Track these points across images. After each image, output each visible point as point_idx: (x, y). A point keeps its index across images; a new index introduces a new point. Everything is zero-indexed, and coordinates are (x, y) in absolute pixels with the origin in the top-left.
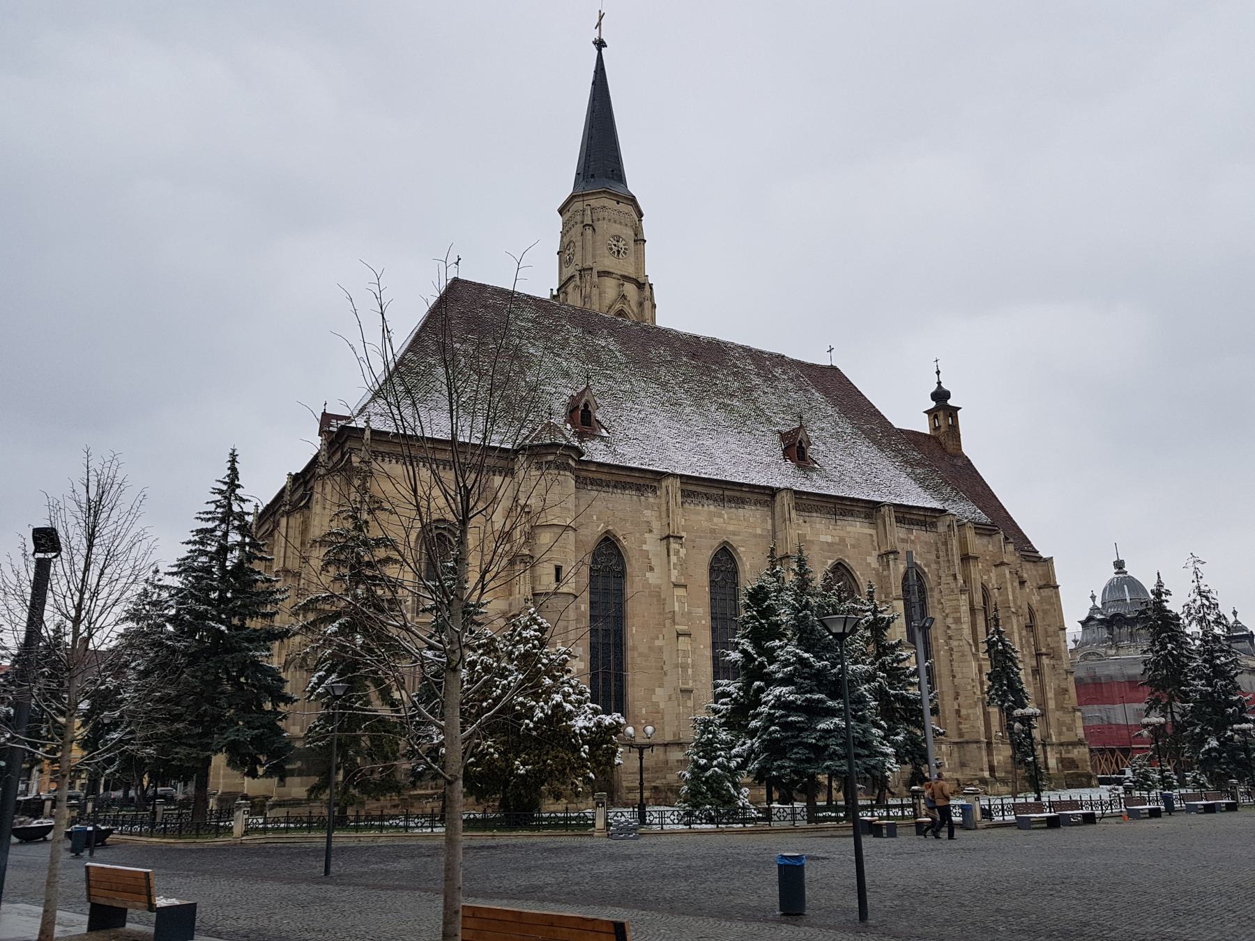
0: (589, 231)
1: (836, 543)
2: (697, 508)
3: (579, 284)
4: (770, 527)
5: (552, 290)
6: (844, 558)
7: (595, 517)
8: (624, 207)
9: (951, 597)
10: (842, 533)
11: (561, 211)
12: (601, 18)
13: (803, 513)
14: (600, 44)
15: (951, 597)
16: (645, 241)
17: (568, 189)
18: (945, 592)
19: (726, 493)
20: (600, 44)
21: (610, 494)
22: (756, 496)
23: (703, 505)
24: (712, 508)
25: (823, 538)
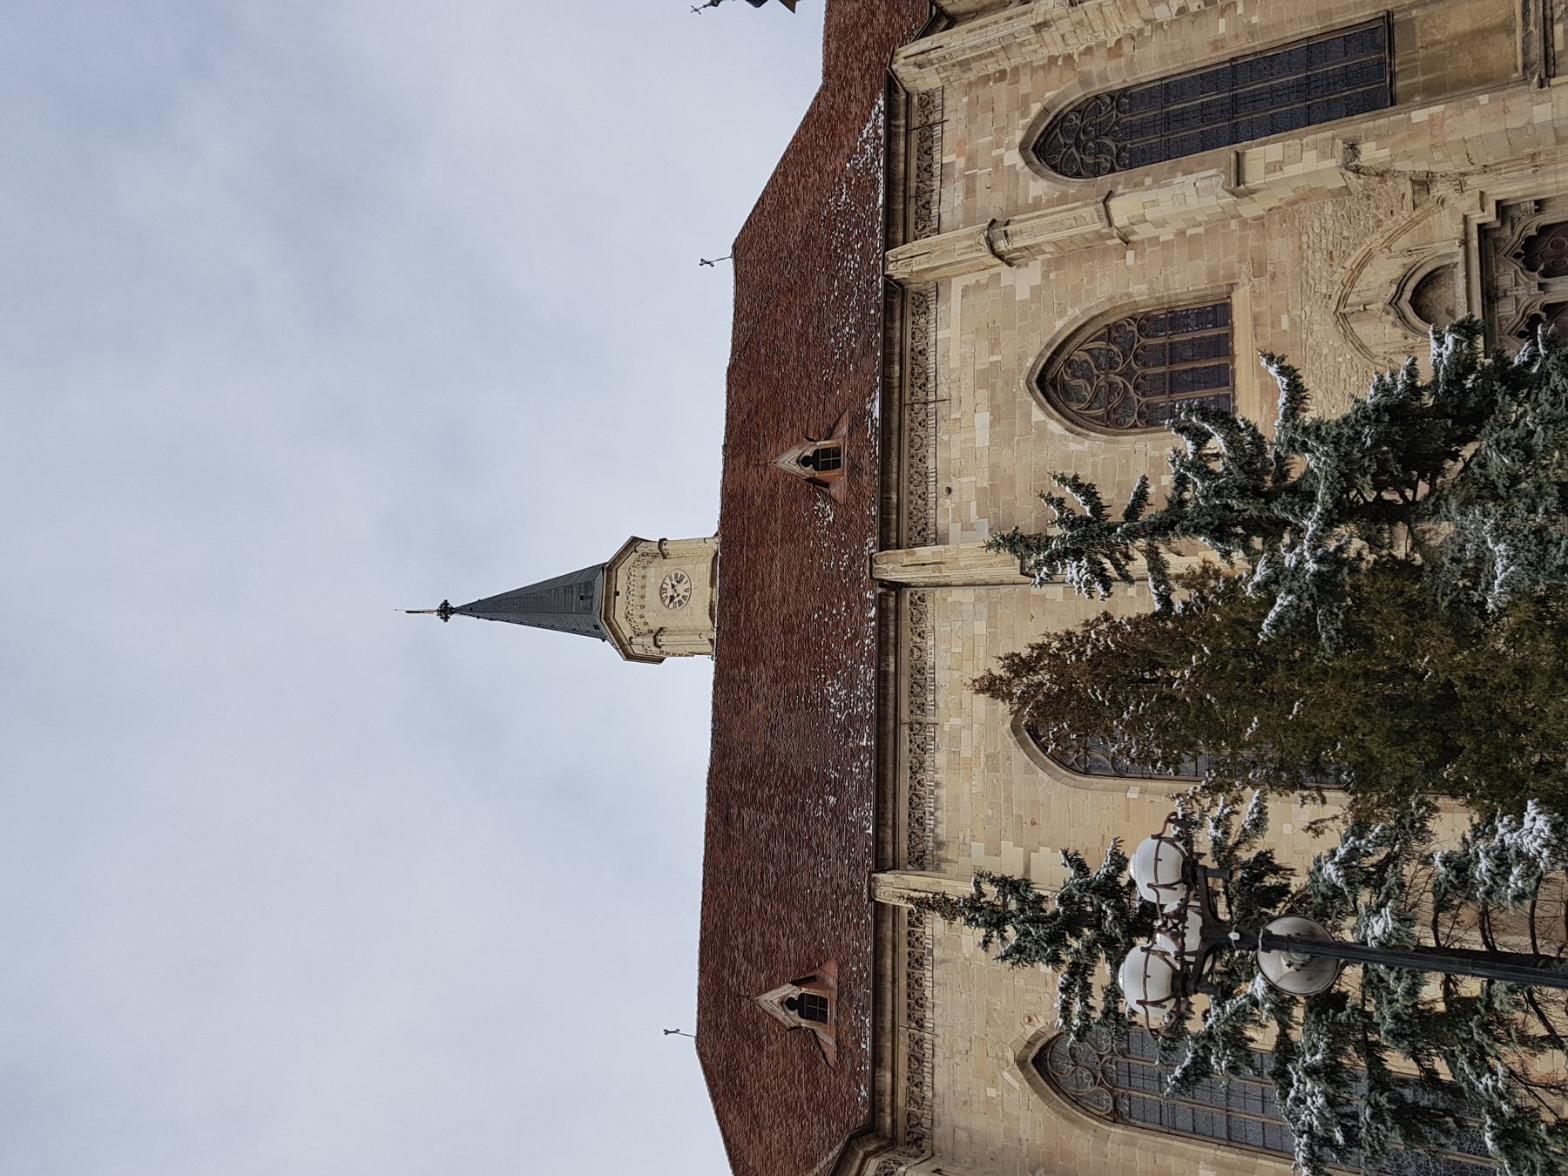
1: (992, 398)
2: (943, 800)
4: (967, 595)
6: (1025, 373)
7: (991, 1092)
9: (1098, 24)
10: (968, 381)
13: (931, 503)
15: (1098, 24)
18: (1087, 40)
19: (905, 715)
21: (938, 1041)
22: (906, 633)
23: (937, 785)
24: (941, 759)
25: (982, 437)
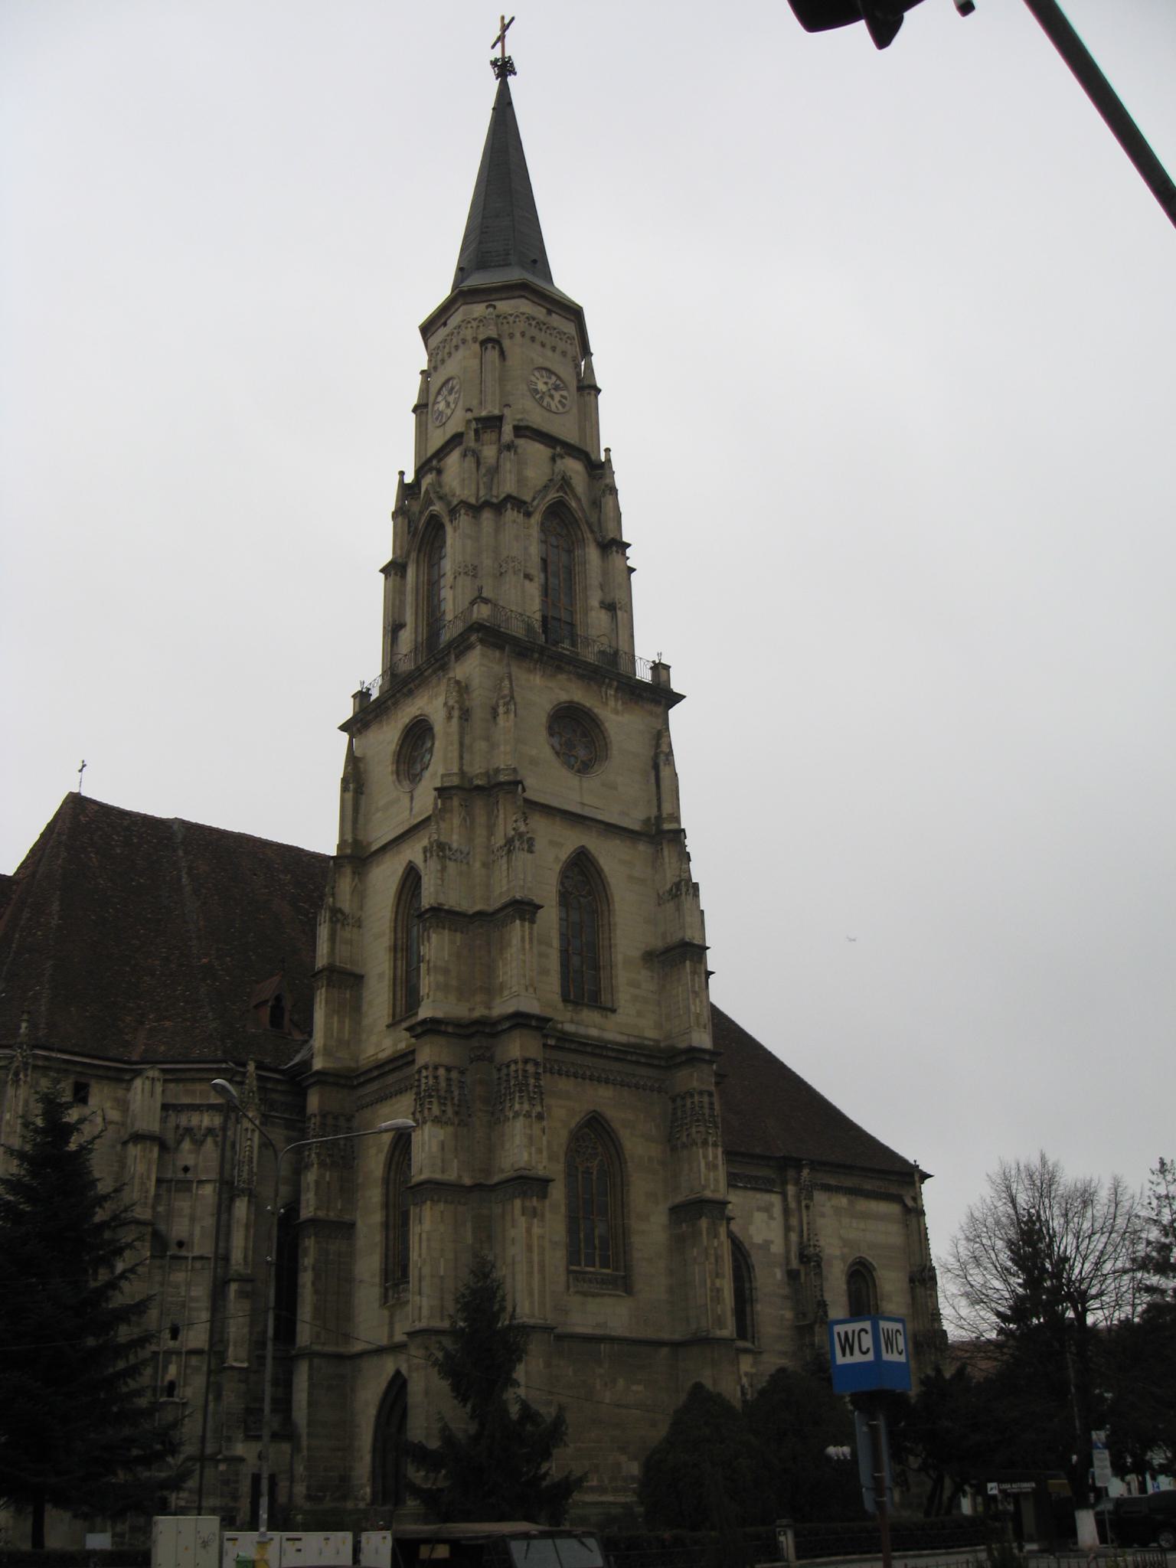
0: (492, 355)
3: (472, 444)
5: (402, 473)
8: (556, 321)
11: (427, 330)
12: (505, 28)
14: (504, 68)
16: (599, 391)
17: (441, 290)
20: (504, 68)
